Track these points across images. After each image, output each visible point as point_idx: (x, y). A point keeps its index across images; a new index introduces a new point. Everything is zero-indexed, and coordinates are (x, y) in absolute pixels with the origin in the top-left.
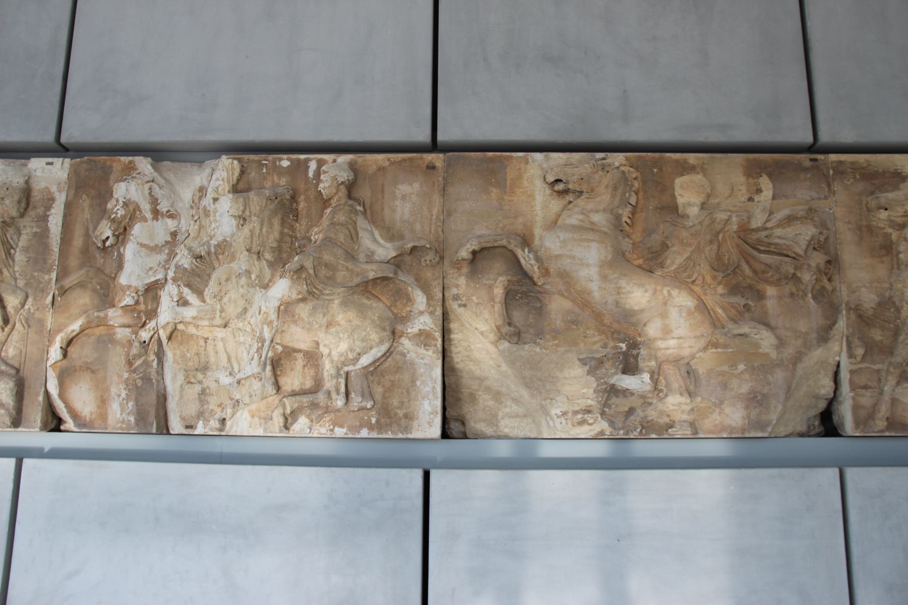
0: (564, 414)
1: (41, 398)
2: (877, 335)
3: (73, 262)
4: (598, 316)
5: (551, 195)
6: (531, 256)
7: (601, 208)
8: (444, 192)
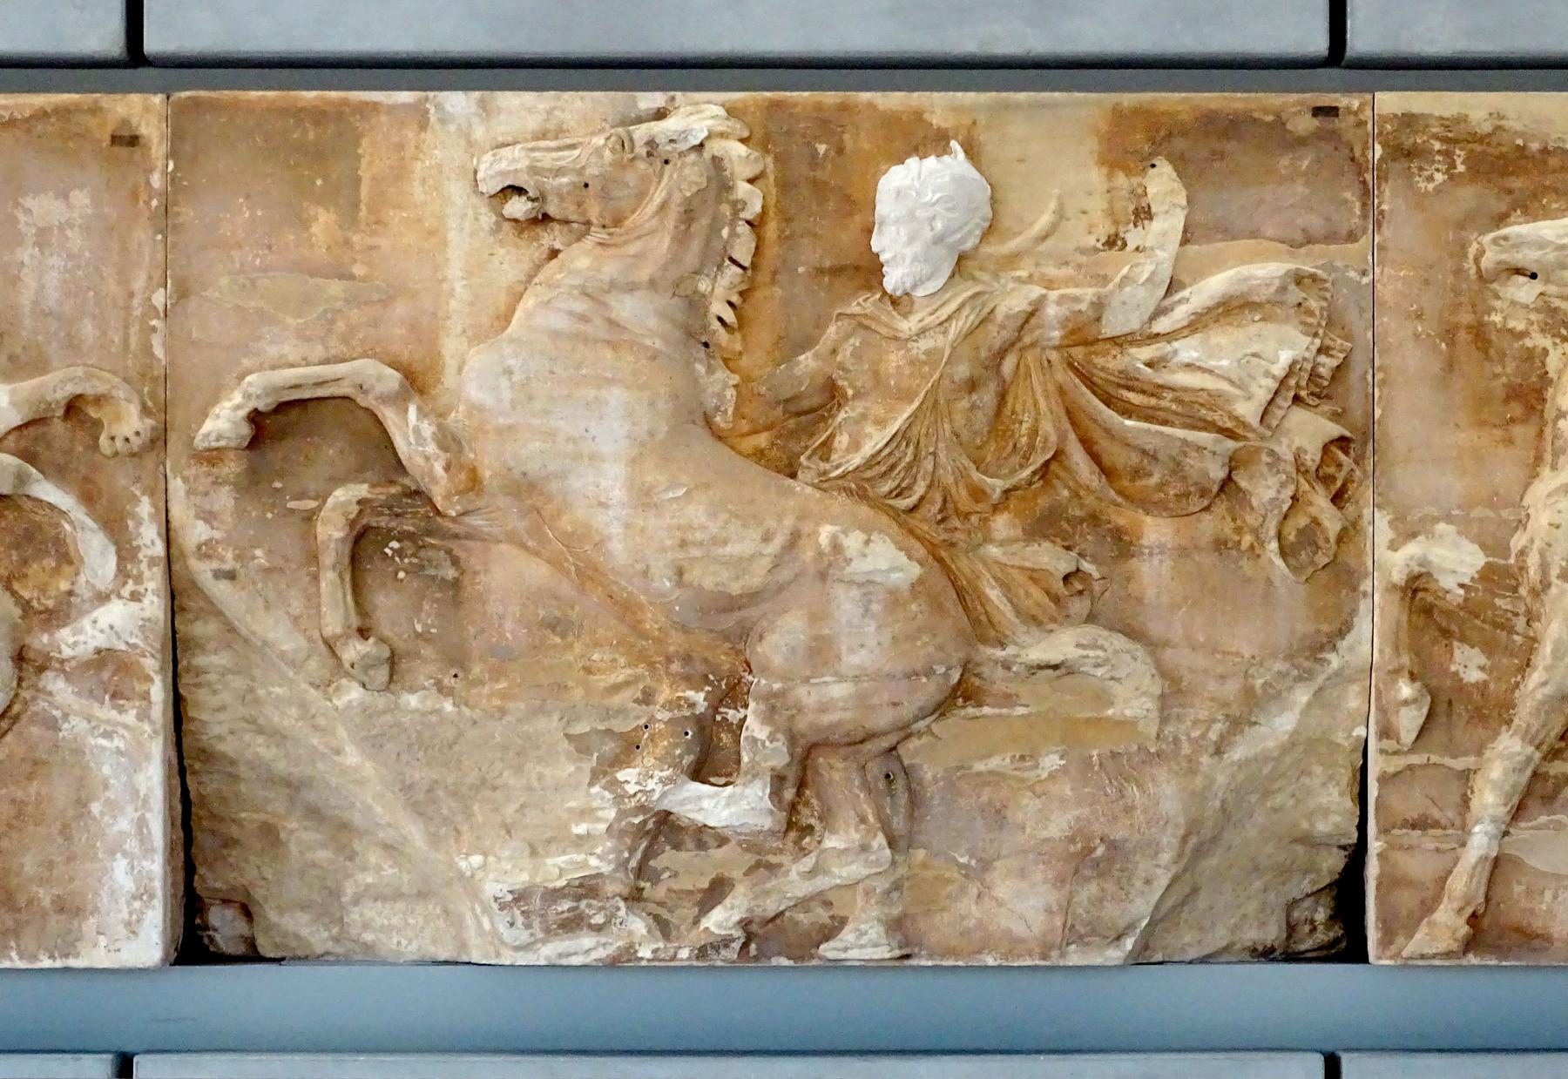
0: (520, 897)
2: (1469, 664)
4: (627, 610)
5: (496, 230)
6: (428, 429)
7: (644, 274)
8: (165, 219)
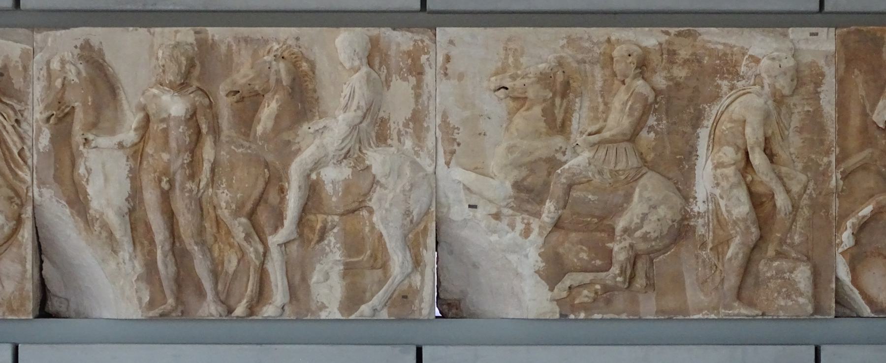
1: (833, 286)
3: (853, 143)
